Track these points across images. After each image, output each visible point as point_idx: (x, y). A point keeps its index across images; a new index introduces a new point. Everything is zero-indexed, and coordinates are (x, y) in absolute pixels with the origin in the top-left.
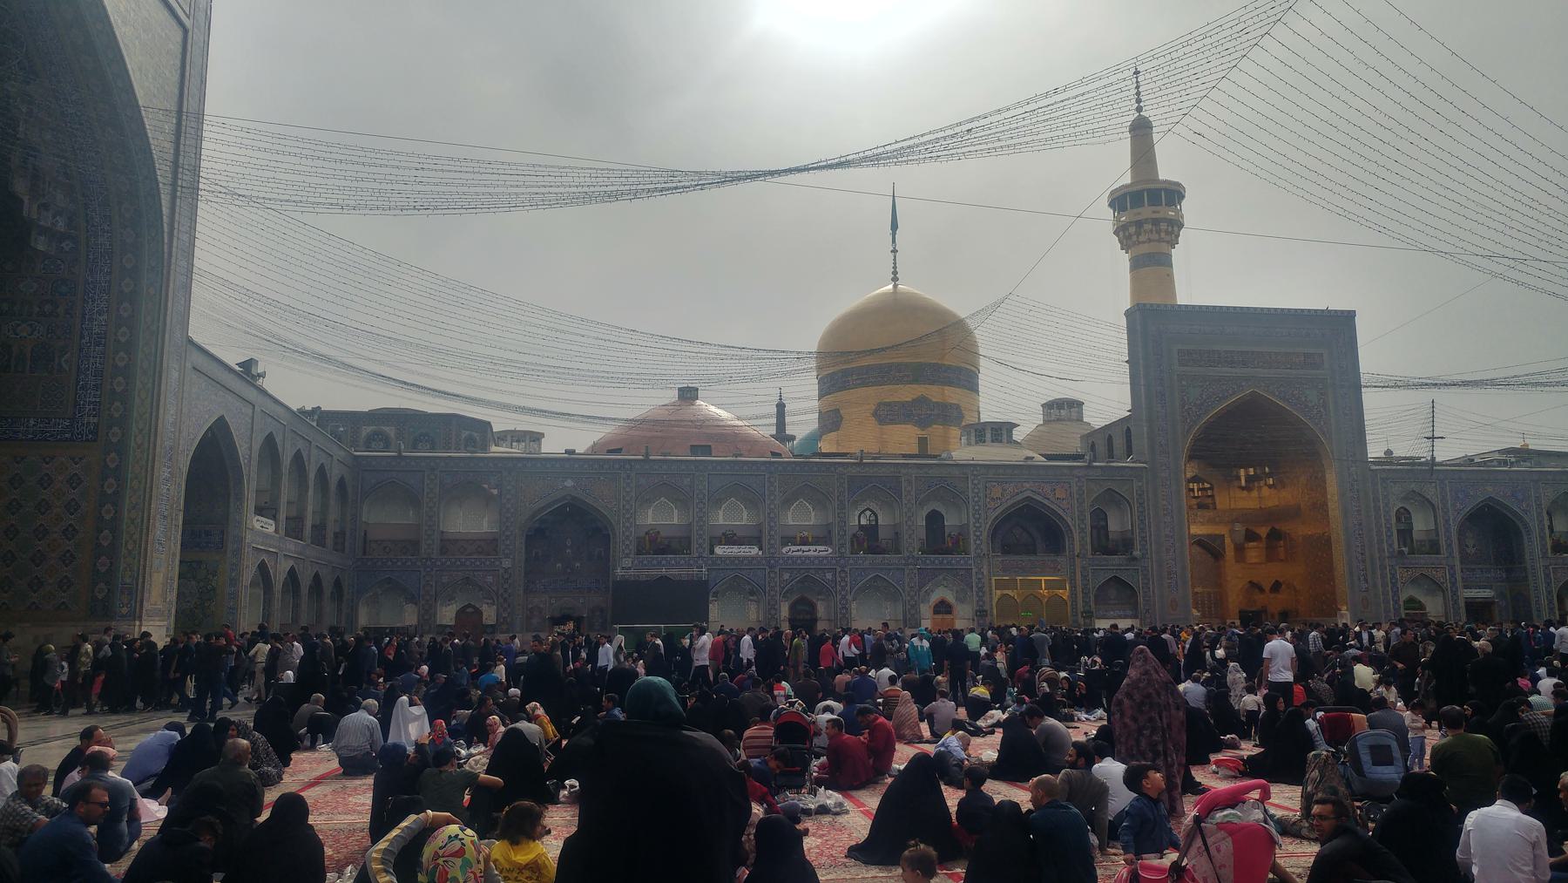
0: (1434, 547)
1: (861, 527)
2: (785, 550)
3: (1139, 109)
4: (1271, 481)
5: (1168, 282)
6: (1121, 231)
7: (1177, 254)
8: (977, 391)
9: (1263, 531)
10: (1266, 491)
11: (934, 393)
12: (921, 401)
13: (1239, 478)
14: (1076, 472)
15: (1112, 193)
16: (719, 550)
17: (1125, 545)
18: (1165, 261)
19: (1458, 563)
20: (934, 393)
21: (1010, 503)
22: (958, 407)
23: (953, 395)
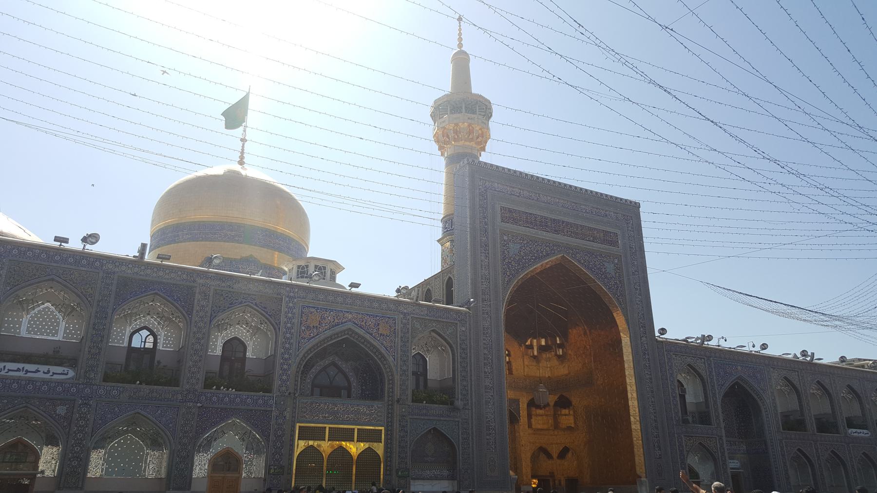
0: (704, 418)
1: (131, 350)
4: (560, 352)
9: (552, 399)
10: (555, 362)
13: (531, 347)
14: (401, 308)
15: (435, 102)
17: (444, 395)
19: (724, 435)
21: (328, 333)
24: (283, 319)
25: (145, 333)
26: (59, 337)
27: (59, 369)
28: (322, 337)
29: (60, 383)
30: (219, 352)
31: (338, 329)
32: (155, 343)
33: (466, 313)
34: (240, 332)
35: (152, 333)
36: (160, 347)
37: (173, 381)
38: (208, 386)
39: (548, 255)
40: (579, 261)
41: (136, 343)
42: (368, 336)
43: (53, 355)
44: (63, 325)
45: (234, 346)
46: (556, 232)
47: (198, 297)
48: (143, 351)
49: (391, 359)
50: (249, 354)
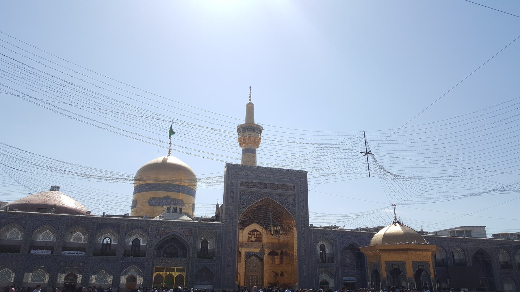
1: (103, 244)
2: (63, 252)
3: (250, 100)
5: (253, 159)
6: (239, 140)
7: (258, 150)
8: (195, 197)
9: (279, 252)
11: (173, 195)
12: (167, 198)
13: (270, 231)
16: (32, 252)
18: (254, 152)
20: (173, 195)
21: (166, 236)
22: (182, 201)
23: (181, 196)
24: (150, 232)
25: (108, 239)
26: (82, 242)
27: (80, 252)
28: (164, 237)
29: (81, 256)
30: (131, 244)
31: (169, 234)
32: (111, 242)
33: (221, 224)
34: (137, 236)
35: (110, 239)
36: (112, 243)
37: (114, 255)
38: (124, 256)
39: (260, 198)
40: (275, 199)
41: (105, 242)
42: (180, 236)
43: (79, 248)
44: (83, 238)
45: (136, 242)
46: (265, 188)
47: (121, 227)
48: (107, 245)
49: (189, 243)
50: (141, 244)
